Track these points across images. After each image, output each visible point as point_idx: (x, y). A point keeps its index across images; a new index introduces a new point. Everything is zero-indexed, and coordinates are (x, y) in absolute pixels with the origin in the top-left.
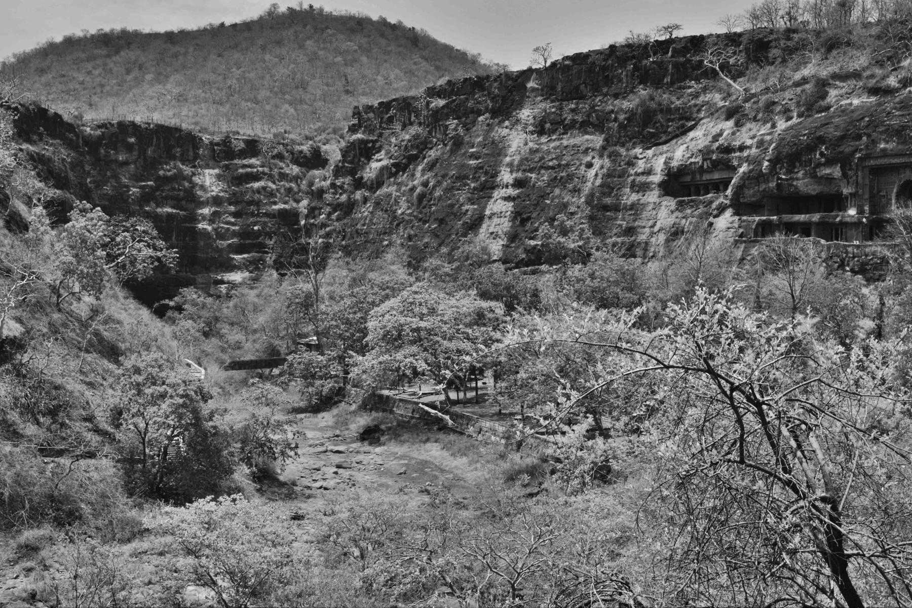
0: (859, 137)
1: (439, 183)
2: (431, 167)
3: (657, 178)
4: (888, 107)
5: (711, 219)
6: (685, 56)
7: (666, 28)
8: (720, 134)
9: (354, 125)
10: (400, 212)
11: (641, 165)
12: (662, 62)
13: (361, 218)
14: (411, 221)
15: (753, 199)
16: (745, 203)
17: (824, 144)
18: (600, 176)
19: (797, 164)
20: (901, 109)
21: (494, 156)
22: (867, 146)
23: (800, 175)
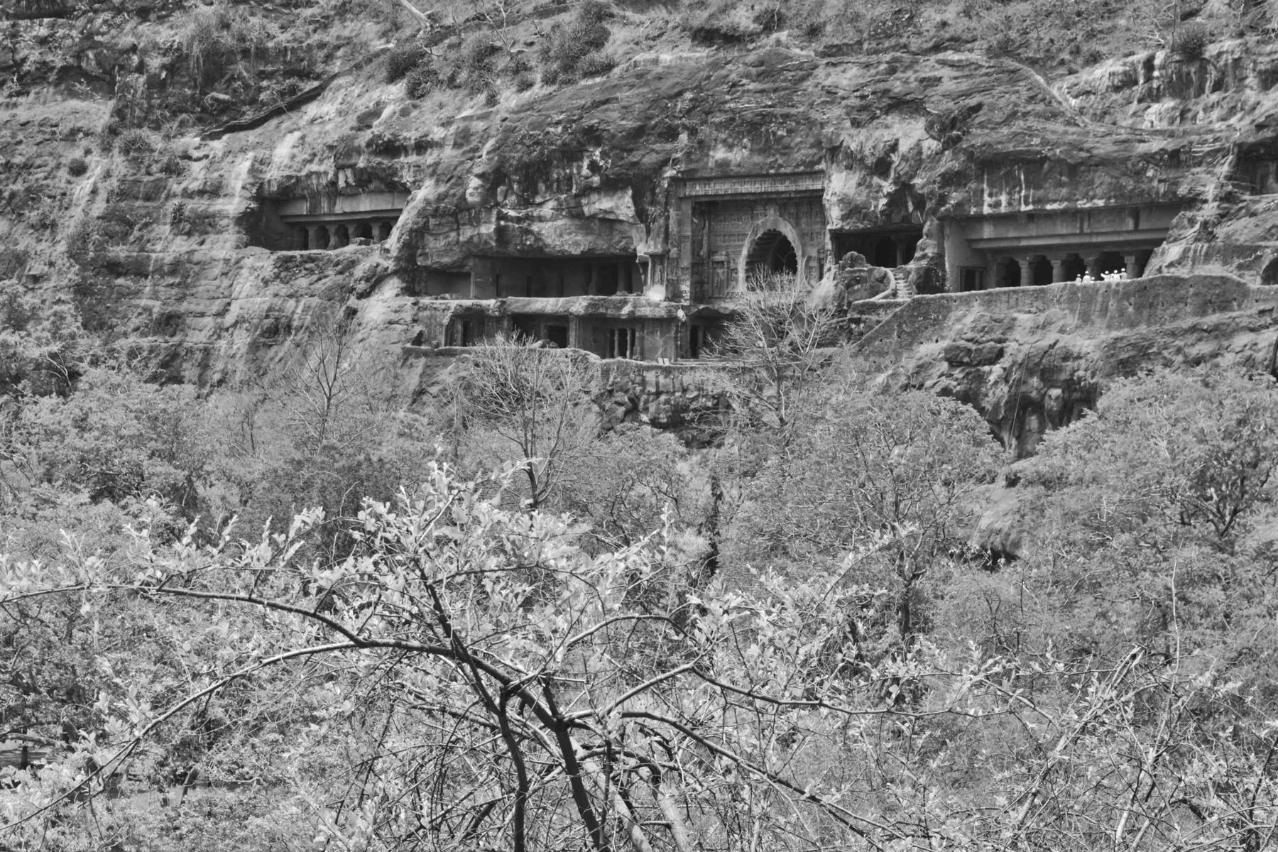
0: (671, 134)
3: (233, 204)
4: (734, 71)
5: (353, 301)
8: (376, 113)
11: (197, 175)
15: (446, 260)
16: (426, 267)
17: (598, 143)
18: (103, 195)
19: (542, 187)
20: (760, 77)
22: (688, 154)
23: (547, 210)
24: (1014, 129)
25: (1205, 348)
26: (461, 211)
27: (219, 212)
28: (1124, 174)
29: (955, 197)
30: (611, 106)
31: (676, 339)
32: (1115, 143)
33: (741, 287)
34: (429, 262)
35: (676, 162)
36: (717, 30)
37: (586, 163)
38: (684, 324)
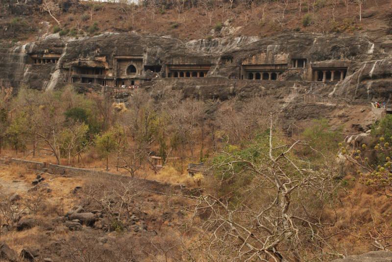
0: (113, 47)
5: (51, 74)
6: (32, 4)
23: (88, 59)
33: (126, 74)
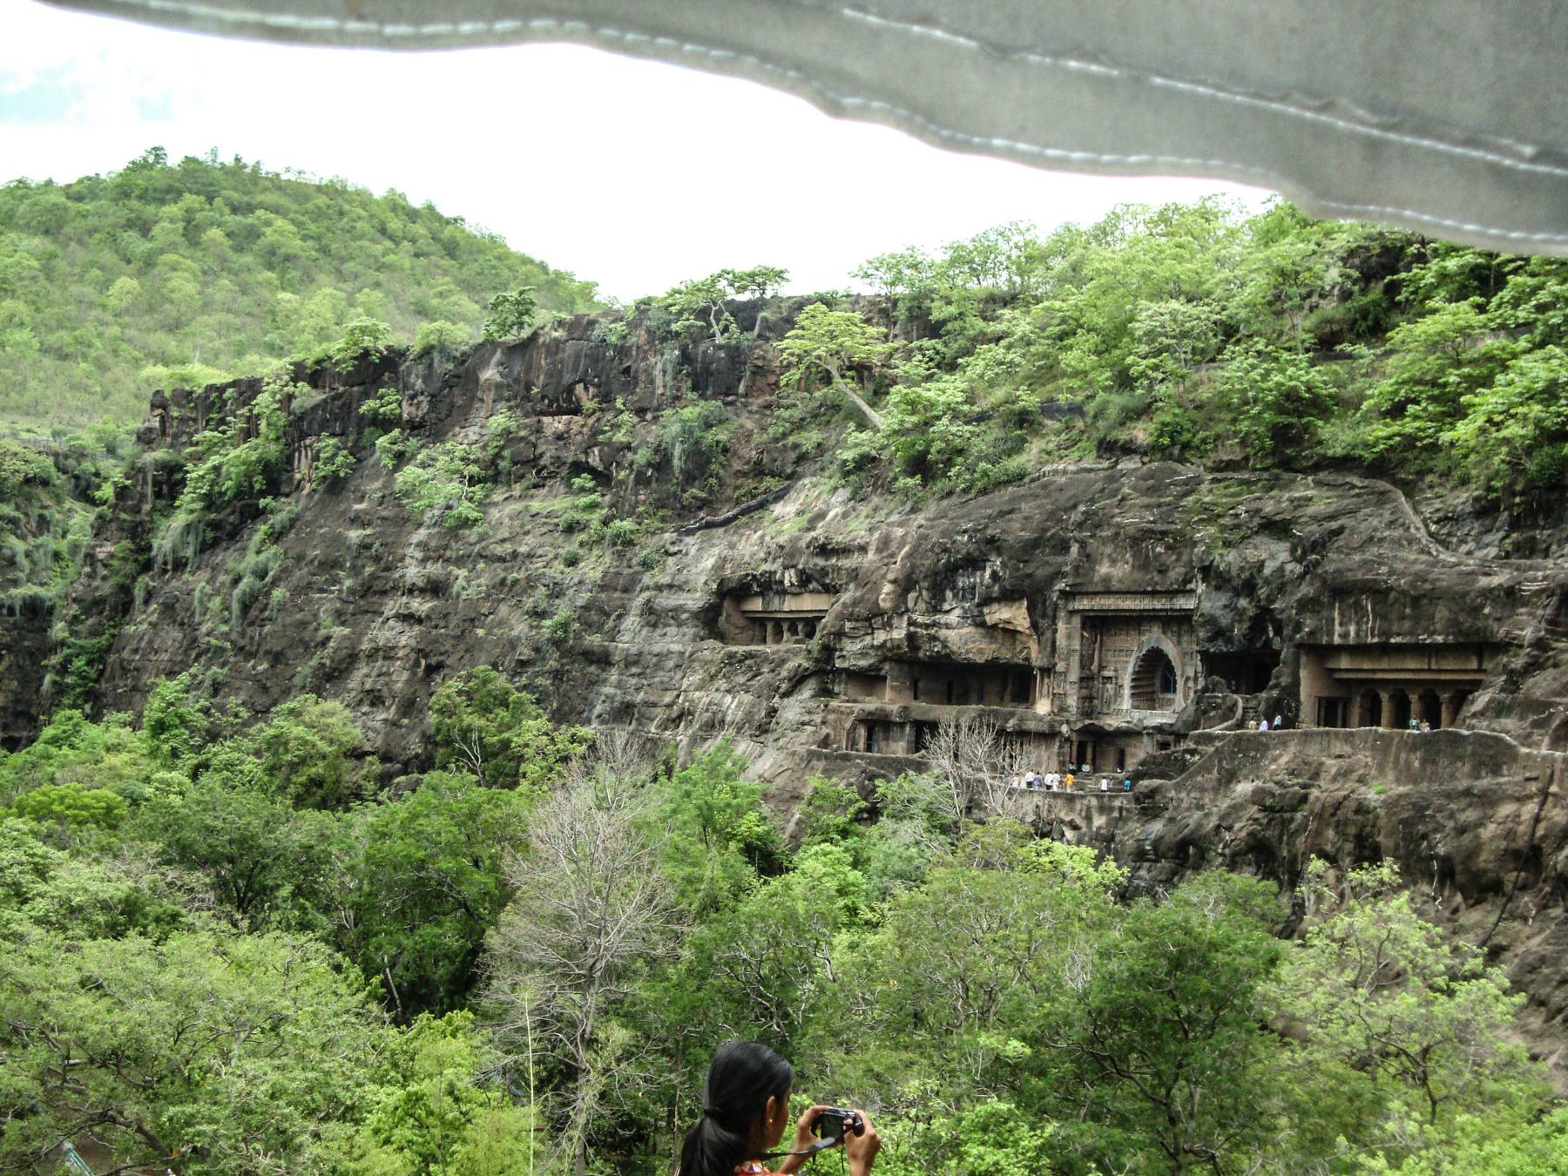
1: (285, 572)
2: (276, 536)
3: (695, 600)
7: (752, 276)
8: (821, 516)
9: (150, 430)
10: (204, 629)
12: (737, 348)
13: (132, 636)
14: (223, 650)
15: (863, 663)
16: (846, 670)
19: (949, 594)
20: (1150, 491)
21: (396, 524)
22: (1077, 568)
23: (953, 618)
24: (1367, 556)
25: (1470, 815)
26: (875, 616)
27: (681, 606)
28: (1462, 610)
29: (1309, 624)
30: (1013, 516)
31: (1059, 754)
32: (1460, 574)
33: (1126, 704)
34: (846, 665)
35: (1064, 575)
36: (1116, 442)
37: (988, 572)
38: (1068, 740)
